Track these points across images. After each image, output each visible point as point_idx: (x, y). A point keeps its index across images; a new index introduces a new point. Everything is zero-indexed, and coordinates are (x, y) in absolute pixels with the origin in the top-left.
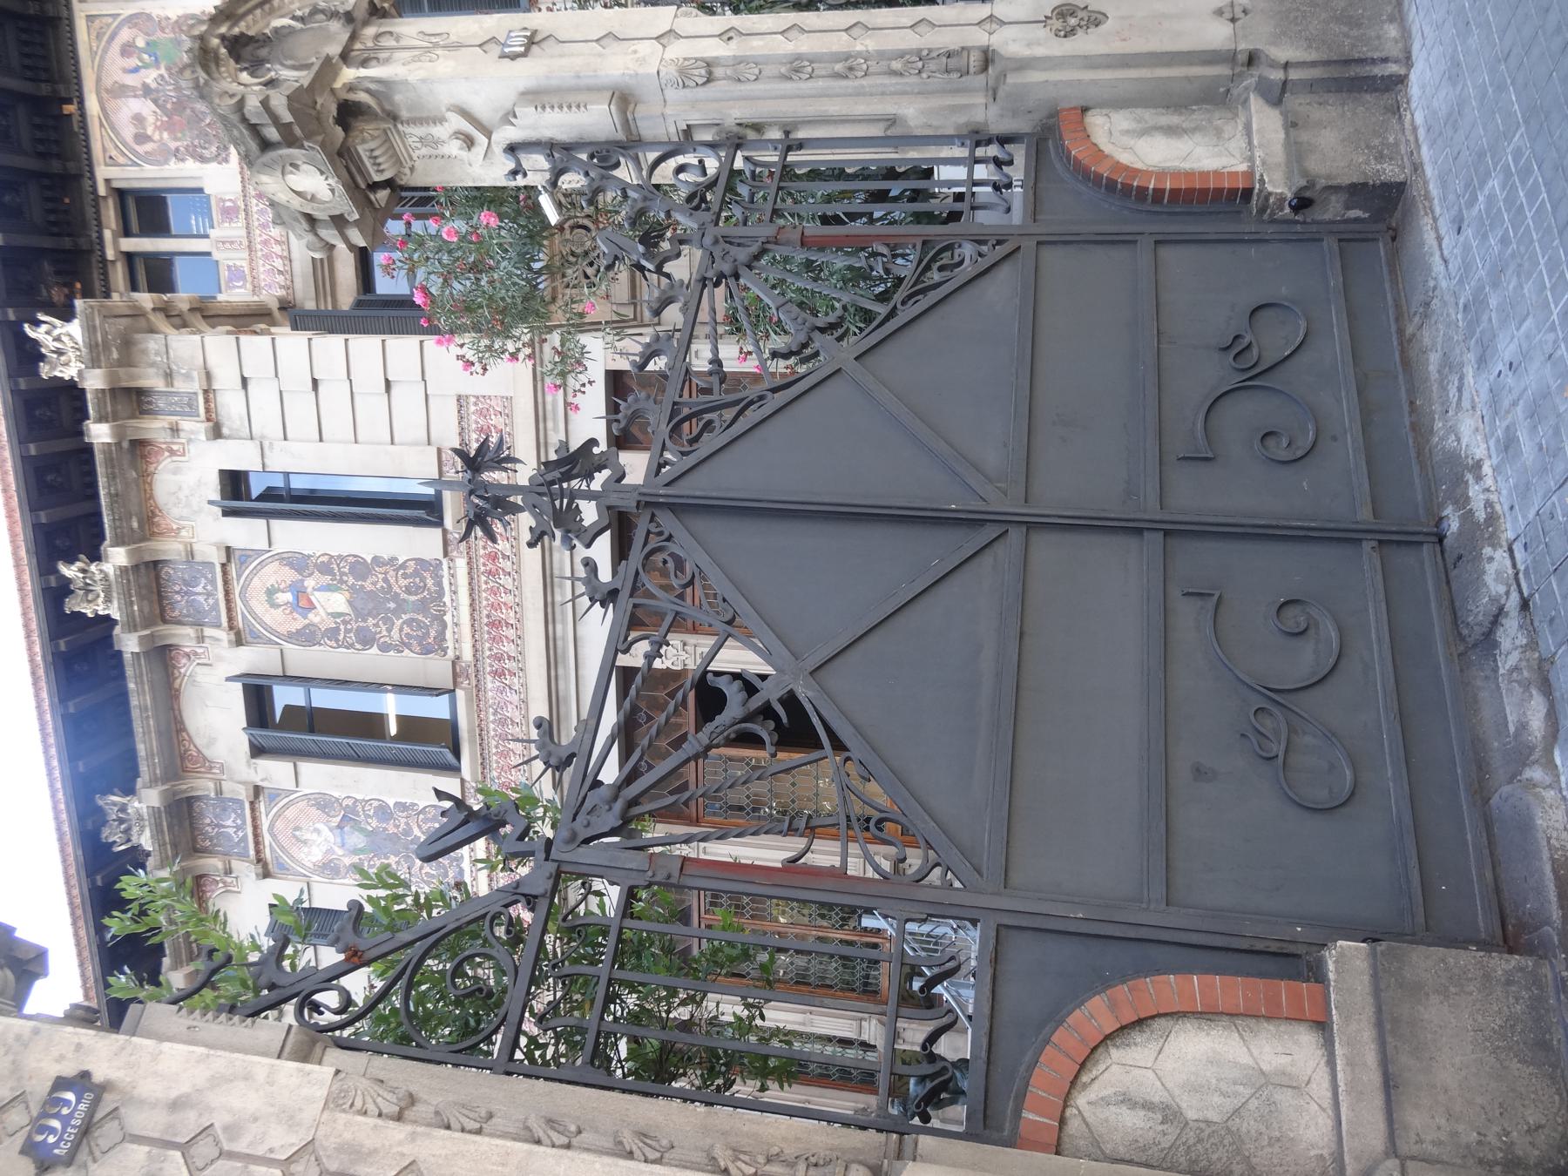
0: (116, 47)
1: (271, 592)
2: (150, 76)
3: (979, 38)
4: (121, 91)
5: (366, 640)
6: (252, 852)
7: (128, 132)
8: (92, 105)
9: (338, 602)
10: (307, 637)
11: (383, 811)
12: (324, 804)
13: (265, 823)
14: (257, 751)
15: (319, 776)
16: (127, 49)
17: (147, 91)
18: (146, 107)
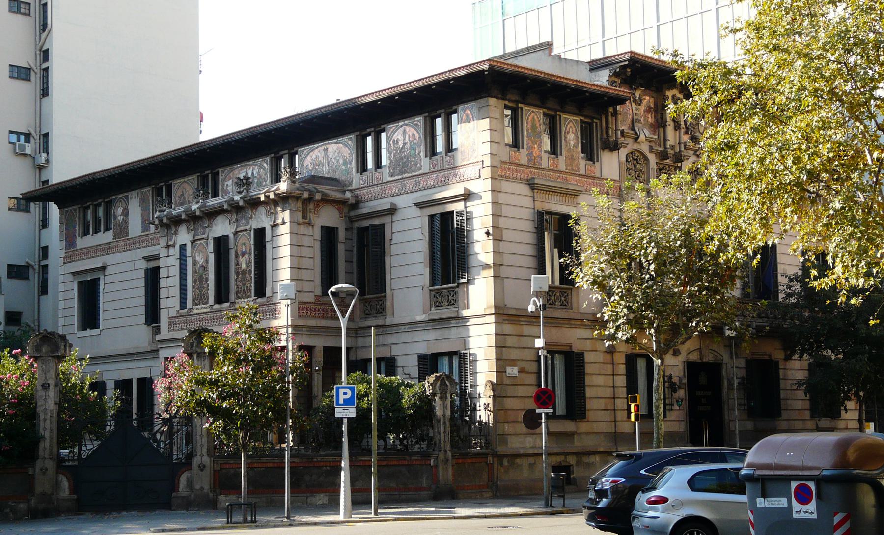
0: (415, 132)
1: (244, 244)
2: (408, 146)
3: (198, 454)
4: (404, 132)
5: (237, 273)
6: (197, 238)
7: (395, 137)
8: (401, 124)
9: (244, 266)
10: (237, 256)
11: (207, 280)
12: (207, 261)
13: (202, 241)
14: (214, 239)
15: (212, 258)
16: (414, 134)
17: (405, 144)
18: (401, 144)
